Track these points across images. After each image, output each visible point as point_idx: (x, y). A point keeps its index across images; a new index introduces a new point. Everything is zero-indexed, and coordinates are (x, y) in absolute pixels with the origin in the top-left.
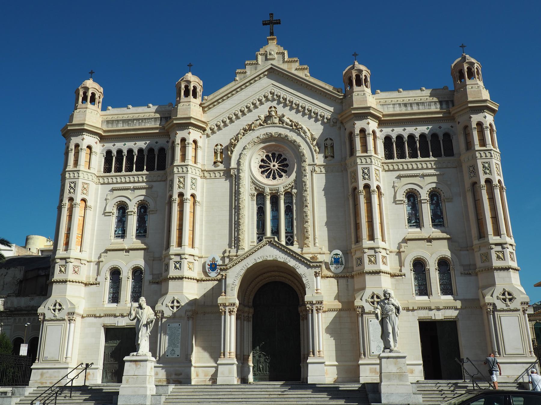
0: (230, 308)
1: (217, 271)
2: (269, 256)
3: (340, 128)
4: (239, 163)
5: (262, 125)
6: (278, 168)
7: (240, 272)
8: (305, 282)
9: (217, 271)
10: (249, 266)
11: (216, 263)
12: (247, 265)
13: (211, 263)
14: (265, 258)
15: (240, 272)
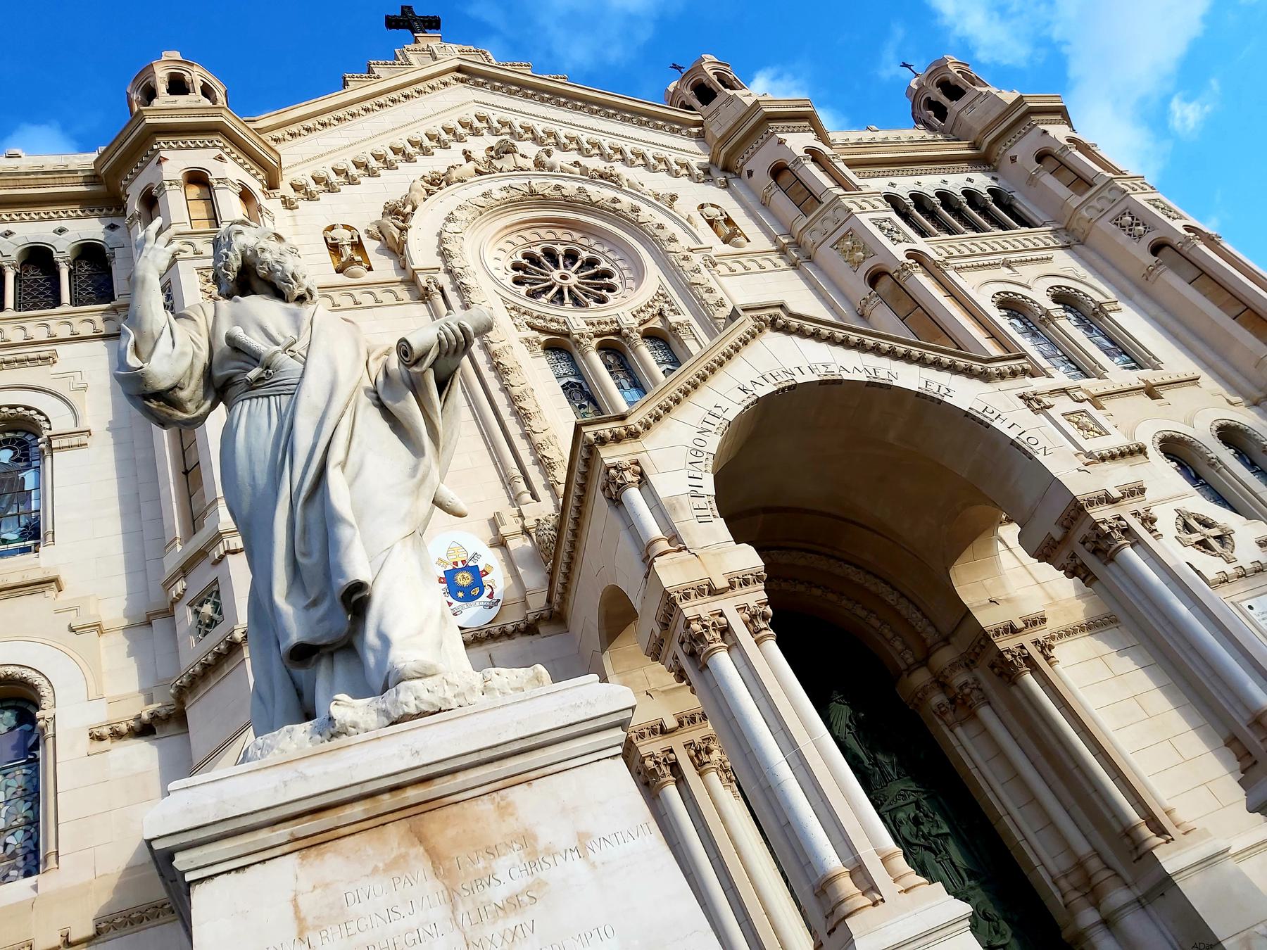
0: (742, 600)
1: (491, 595)
2: (797, 372)
3: (727, 181)
4: (444, 254)
5: (481, 173)
6: (570, 291)
7: (702, 443)
8: (1012, 434)
9: (491, 595)
10: (731, 416)
11: (471, 564)
12: (718, 412)
13: (450, 567)
14: (785, 381)
15: (702, 443)
